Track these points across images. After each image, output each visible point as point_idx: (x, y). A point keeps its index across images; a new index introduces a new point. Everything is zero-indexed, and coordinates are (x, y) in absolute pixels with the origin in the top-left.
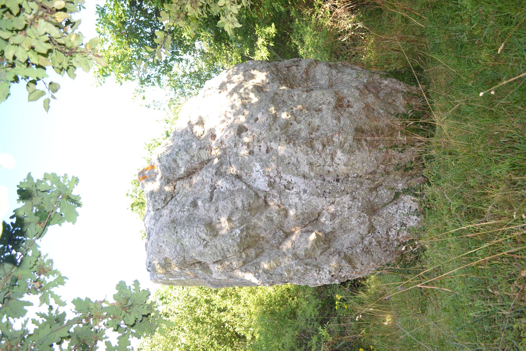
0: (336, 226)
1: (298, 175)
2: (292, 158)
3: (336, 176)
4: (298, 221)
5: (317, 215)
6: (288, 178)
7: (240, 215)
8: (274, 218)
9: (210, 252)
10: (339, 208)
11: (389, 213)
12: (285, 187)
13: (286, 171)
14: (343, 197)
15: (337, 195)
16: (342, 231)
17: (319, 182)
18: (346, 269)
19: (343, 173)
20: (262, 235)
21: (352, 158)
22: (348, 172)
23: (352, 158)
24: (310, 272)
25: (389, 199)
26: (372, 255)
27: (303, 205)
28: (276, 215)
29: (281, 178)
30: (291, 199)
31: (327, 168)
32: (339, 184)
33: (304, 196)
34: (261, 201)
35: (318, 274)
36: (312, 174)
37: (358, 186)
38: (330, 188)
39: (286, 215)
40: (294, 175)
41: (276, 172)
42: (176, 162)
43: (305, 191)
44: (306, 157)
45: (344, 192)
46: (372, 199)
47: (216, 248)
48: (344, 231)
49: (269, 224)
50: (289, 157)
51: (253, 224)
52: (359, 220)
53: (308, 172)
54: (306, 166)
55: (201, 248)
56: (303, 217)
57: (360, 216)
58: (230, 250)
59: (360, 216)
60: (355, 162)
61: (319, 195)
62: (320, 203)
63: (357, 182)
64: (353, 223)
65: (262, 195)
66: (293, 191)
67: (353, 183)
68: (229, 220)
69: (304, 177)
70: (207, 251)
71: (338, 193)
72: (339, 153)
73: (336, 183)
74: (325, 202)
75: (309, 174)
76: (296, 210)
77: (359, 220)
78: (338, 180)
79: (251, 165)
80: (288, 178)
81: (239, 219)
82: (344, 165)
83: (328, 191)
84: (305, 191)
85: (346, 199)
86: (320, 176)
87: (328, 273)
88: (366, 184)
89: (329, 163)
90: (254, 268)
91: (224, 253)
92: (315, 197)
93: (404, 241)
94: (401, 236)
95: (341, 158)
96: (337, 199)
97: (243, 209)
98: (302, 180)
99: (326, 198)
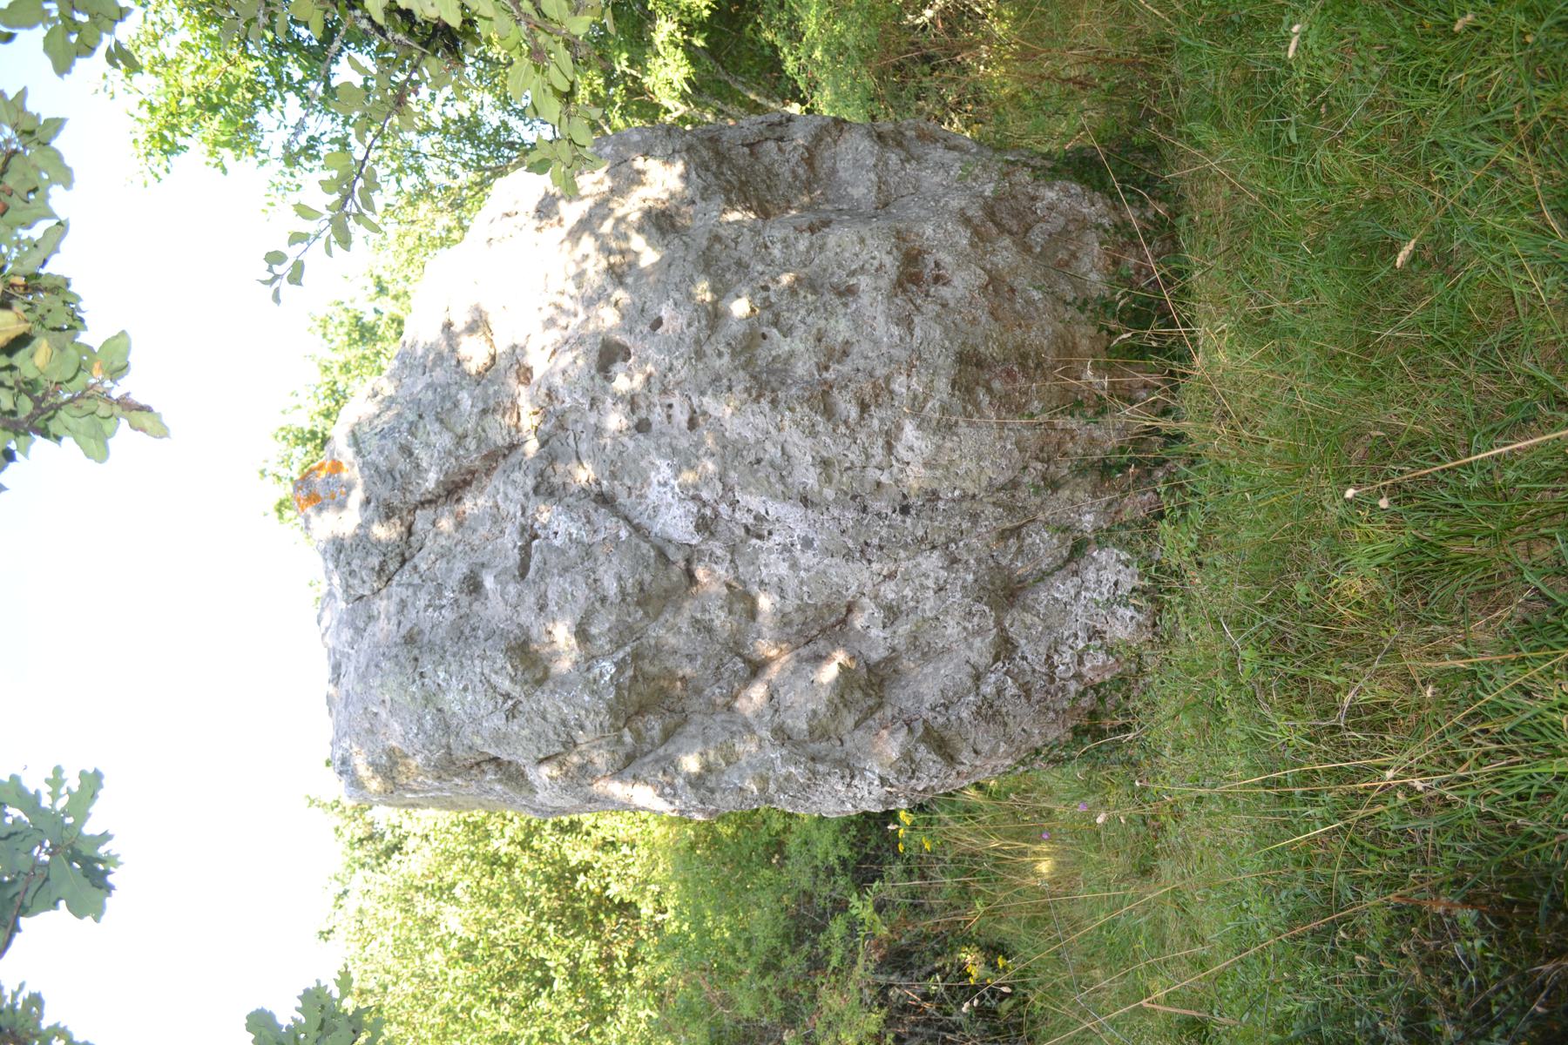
0: (901, 643)
1: (786, 498)
2: (768, 445)
4: (788, 630)
5: (844, 611)
6: (754, 501)
7: (613, 618)
8: (717, 623)
9: (525, 732)
10: (908, 592)
11: (1056, 600)
14: (920, 559)
15: (902, 554)
17: (851, 515)
21: (949, 444)
22: (935, 485)
23: (949, 444)
24: (826, 781)
25: (1055, 559)
26: (1006, 724)
27: (802, 583)
28: (723, 615)
29: (734, 504)
30: (766, 565)
31: (873, 474)
32: (909, 521)
34: (677, 572)
35: (849, 785)
36: (829, 493)
38: (884, 533)
39: (753, 613)
40: (775, 497)
41: (719, 487)
42: (411, 454)
43: (807, 543)
44: (809, 442)
45: (924, 544)
46: (1004, 562)
47: (544, 718)
48: (924, 654)
50: (758, 441)
51: (653, 642)
53: (816, 488)
54: (812, 469)
55: (498, 721)
57: (970, 613)
58: (587, 723)
59: (970, 613)
60: (955, 457)
61: (848, 555)
62: (855, 577)
64: (949, 631)
65: (678, 557)
66: (770, 543)
67: (949, 518)
68: (582, 634)
69: (805, 501)
71: (905, 546)
72: (910, 432)
74: (867, 574)
75: (820, 493)
76: (782, 597)
78: (905, 510)
79: (643, 464)
80: (754, 501)
83: (875, 541)
84: (807, 543)
85: (931, 562)
86: (854, 498)
89: (878, 458)
91: (568, 734)
92: (837, 560)
93: (1098, 680)
94: (1088, 665)
95: (916, 444)
97: (623, 600)
98: (799, 511)
99: (870, 562)
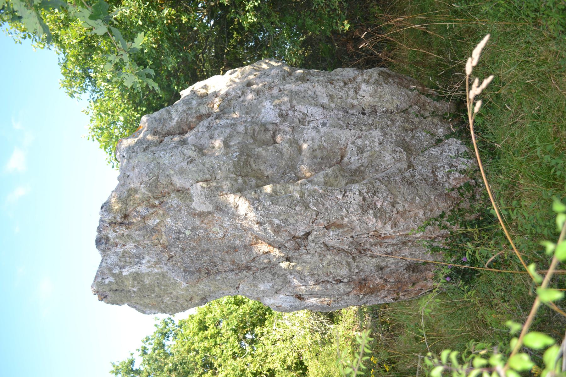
0: (365, 161)
1: (315, 105)
2: (309, 92)
3: (361, 109)
4: (315, 160)
5: (340, 157)
6: (303, 108)
7: (240, 139)
8: (285, 150)
9: (195, 169)
10: (367, 142)
11: (432, 154)
12: (299, 121)
13: (301, 101)
14: (371, 131)
15: (364, 128)
16: (373, 170)
17: (341, 113)
18: (382, 193)
19: (369, 105)
20: (266, 174)
21: (379, 90)
22: (375, 104)
23: (379, 90)
24: (333, 193)
25: (429, 143)
26: (418, 190)
27: (321, 137)
28: (287, 145)
29: (295, 111)
30: (306, 134)
31: (350, 101)
32: (365, 117)
33: (323, 130)
34: (269, 135)
35: (344, 195)
36: (333, 105)
37: (389, 123)
38: (356, 120)
39: (300, 150)
40: (311, 105)
41: (289, 105)
42: (169, 113)
43: (324, 125)
44: (325, 89)
45: (371, 126)
46: (408, 140)
47: (204, 165)
48: (376, 170)
49: (278, 157)
50: (305, 91)
51: (256, 153)
52: (394, 155)
53: (328, 103)
54: (326, 97)
55: (184, 164)
56: (321, 155)
57: (395, 151)
58: (223, 168)
59: (395, 151)
60: (382, 94)
61: (341, 128)
62: (345, 136)
63: (388, 118)
64: (386, 159)
65: (270, 127)
66: (309, 127)
67: (382, 118)
68: (226, 144)
69: (323, 106)
70: (191, 167)
71: (365, 125)
72: (363, 86)
73: (362, 116)
74: (349, 134)
75: (329, 105)
76: (313, 142)
77: (394, 155)
78: (364, 114)
79: (259, 107)
80: (303, 108)
81: (238, 143)
82: (370, 96)
83: (352, 123)
84: (324, 125)
85: (376, 133)
86: (343, 108)
87: (357, 193)
88: (398, 121)
89: (352, 95)
90: (253, 193)
91: (213, 172)
92: (337, 129)
93: (458, 186)
94: (452, 178)
95: (366, 89)
96: (364, 133)
97: (246, 133)
98: (320, 110)
99: (350, 130)
